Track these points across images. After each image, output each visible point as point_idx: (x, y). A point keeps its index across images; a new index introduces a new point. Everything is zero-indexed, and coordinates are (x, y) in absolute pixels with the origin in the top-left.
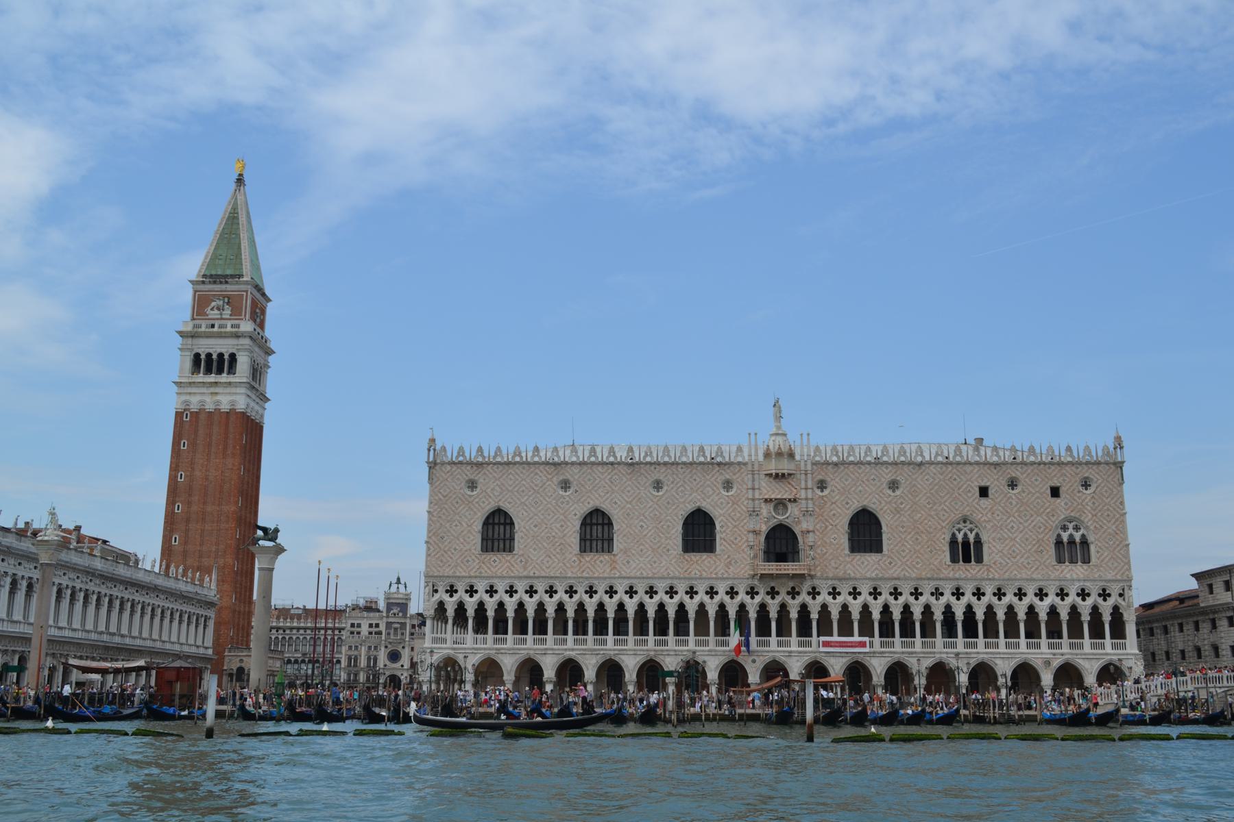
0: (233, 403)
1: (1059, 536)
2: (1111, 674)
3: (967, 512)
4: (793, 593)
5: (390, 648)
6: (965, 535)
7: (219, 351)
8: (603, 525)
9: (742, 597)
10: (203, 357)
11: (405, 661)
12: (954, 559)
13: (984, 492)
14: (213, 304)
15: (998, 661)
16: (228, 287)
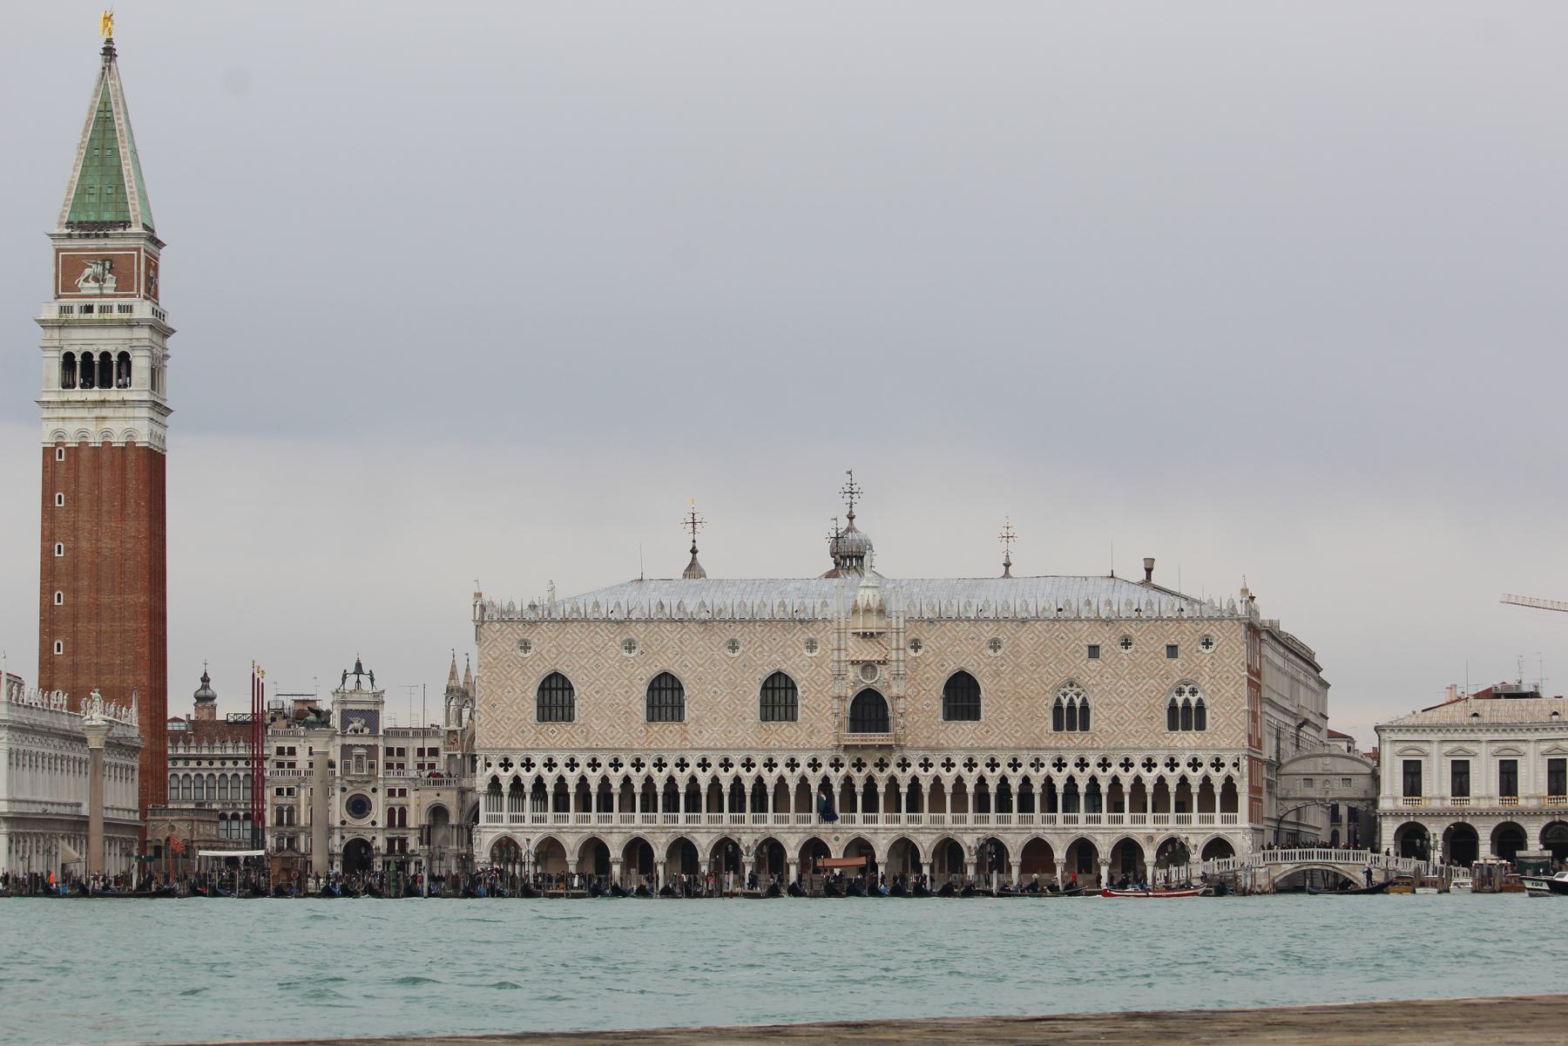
0: (129, 433)
1: (1173, 700)
2: (1218, 848)
3: (1073, 674)
4: (882, 765)
5: (352, 791)
6: (1071, 700)
7: (103, 349)
8: (673, 689)
9: (825, 769)
10: (78, 359)
11: (378, 814)
12: (1058, 727)
13: (1094, 651)
14: (88, 271)
15: (1099, 837)
16: (109, 243)
